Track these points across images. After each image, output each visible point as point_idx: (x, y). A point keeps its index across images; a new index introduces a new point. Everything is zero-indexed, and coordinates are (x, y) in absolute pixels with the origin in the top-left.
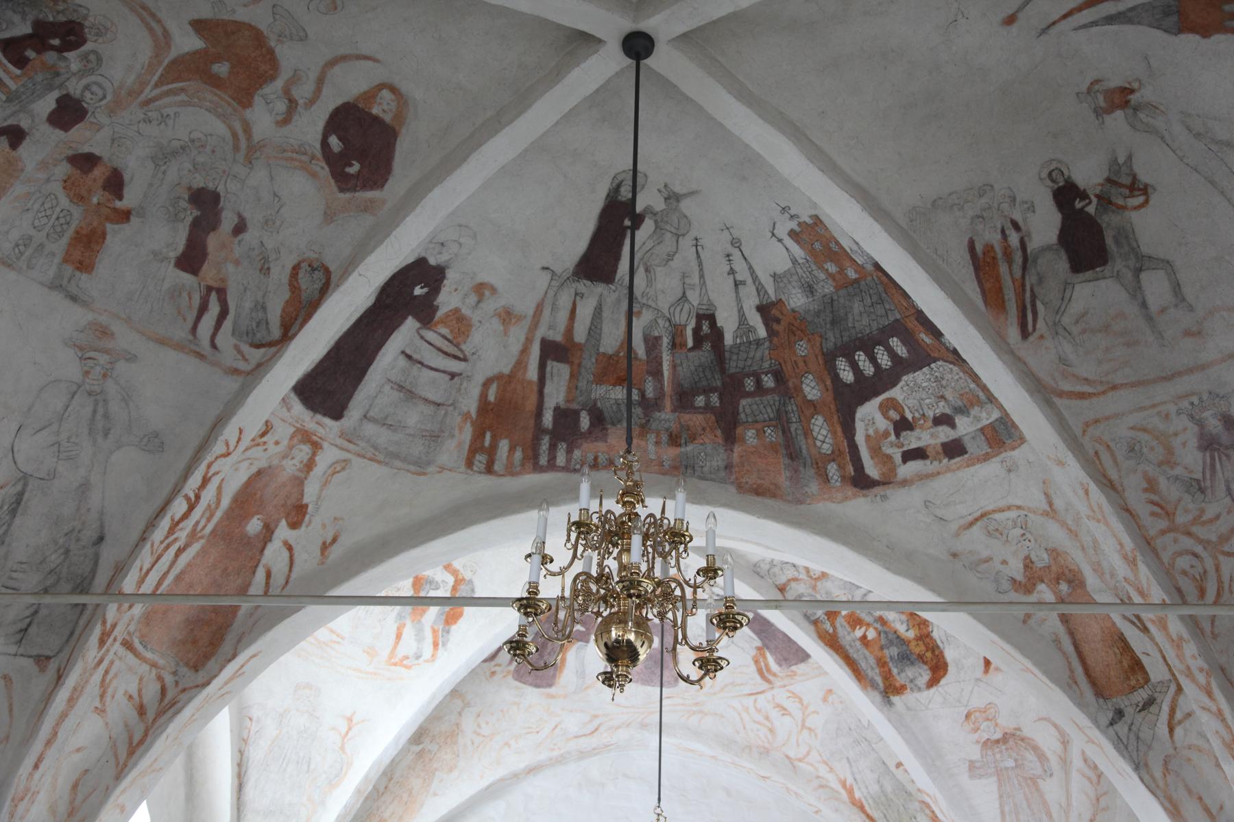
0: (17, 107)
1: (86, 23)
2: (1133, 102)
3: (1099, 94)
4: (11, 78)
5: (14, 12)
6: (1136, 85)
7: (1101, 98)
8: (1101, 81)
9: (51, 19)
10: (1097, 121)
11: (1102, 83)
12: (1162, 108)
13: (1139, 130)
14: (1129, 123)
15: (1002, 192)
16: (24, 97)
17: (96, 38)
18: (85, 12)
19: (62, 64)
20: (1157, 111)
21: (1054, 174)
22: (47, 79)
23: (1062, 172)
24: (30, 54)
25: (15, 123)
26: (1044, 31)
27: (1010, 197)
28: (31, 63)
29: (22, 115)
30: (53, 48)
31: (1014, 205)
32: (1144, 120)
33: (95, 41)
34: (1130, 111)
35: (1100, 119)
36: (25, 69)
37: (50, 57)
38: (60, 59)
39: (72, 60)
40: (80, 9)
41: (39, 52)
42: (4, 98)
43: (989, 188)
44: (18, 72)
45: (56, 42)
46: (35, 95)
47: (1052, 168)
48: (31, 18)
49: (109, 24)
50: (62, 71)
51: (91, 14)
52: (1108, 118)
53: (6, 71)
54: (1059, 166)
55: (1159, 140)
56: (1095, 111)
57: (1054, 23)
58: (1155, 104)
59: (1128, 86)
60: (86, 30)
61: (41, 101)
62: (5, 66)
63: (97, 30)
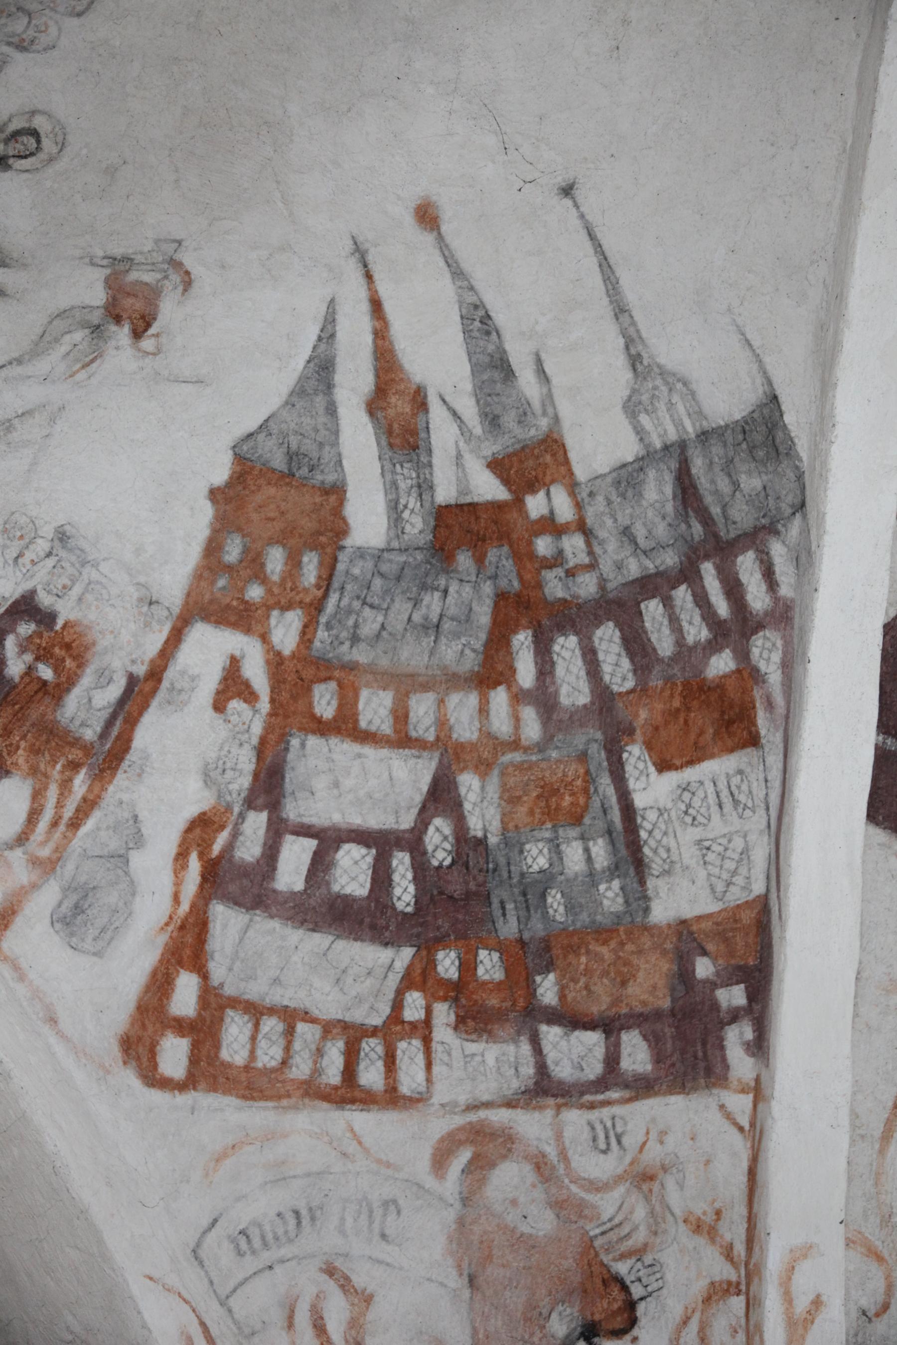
2: (113, 328)
3: (159, 276)
6: (147, 344)
7: (148, 277)
8: (185, 290)
10: (101, 253)
11: (181, 288)
12: (82, 375)
13: (50, 322)
14: (73, 308)
15: (53, 30)
20: (78, 366)
21: (31, 142)
23: (26, 157)
26: (360, 253)
27: (32, 42)
31: (9, 44)
32: (67, 337)
34: (96, 317)
35: (105, 262)
43: (79, 8)
47: (46, 143)
52: (98, 275)
54: (42, 156)
55: (15, 355)
56: (127, 259)
57: (369, 276)
58: (94, 365)
59: (151, 331)
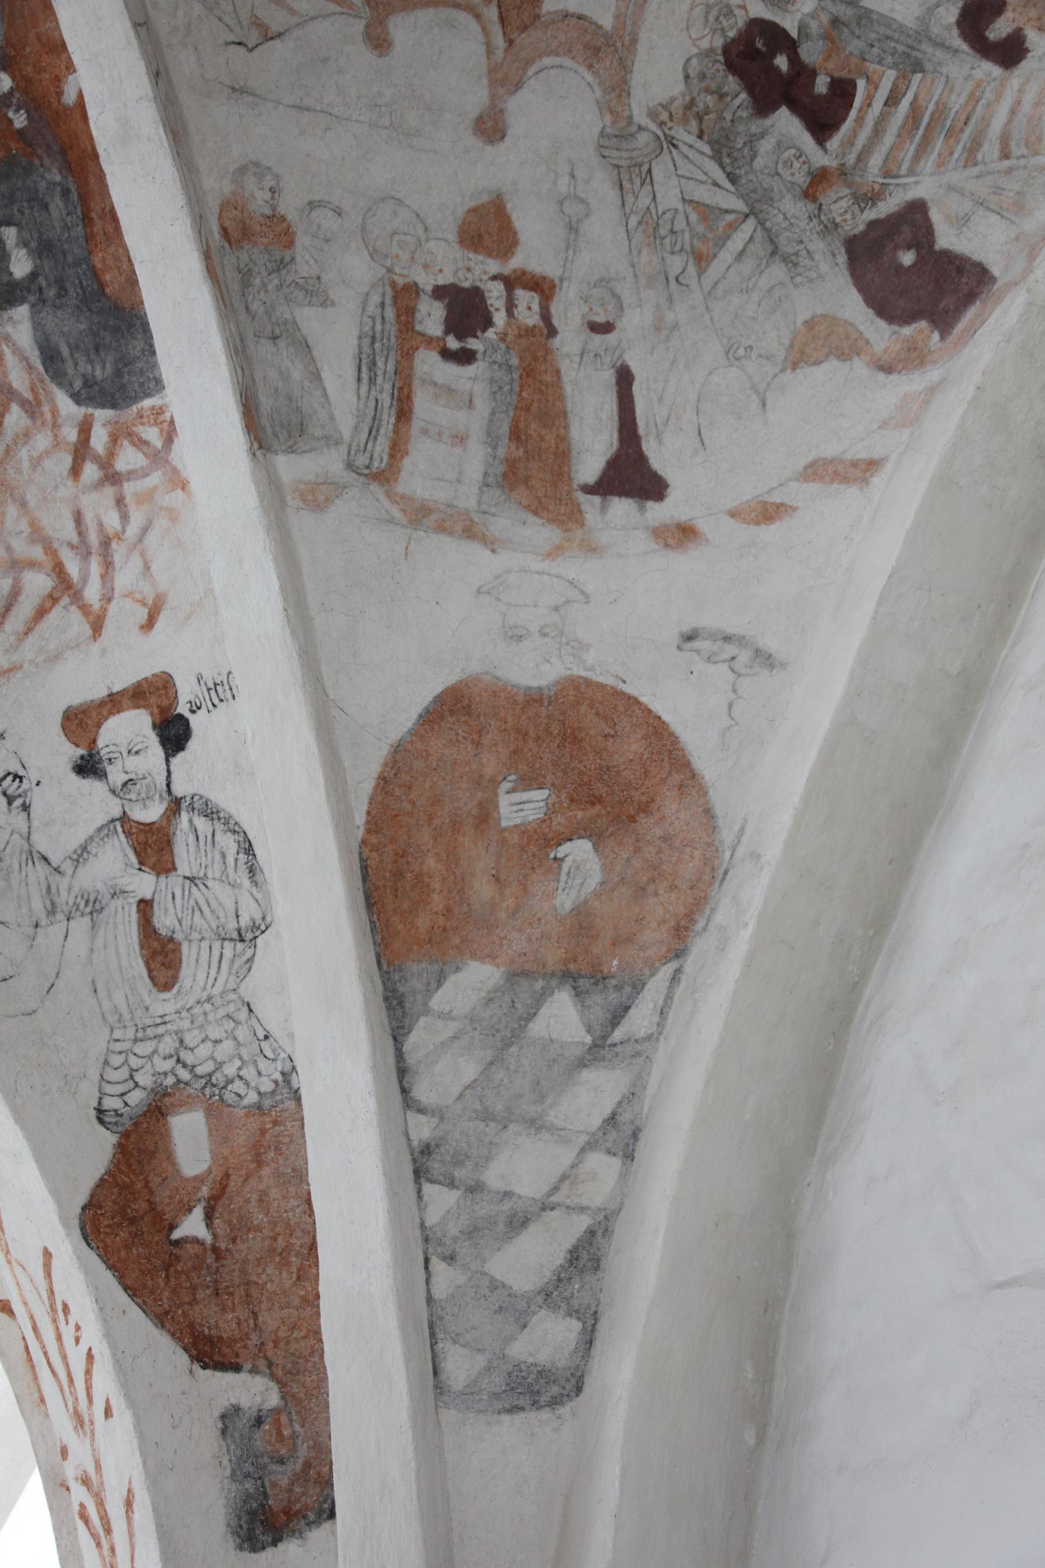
0: (924, 46)
1: (719, 42)
4: (876, 88)
5: (754, 156)
9: (743, 96)
16: (900, 48)
17: (736, 11)
18: (694, 62)
19: (814, 26)
22: (852, 33)
24: (821, 85)
25: (955, 32)
28: (836, 75)
29: (935, 30)
30: (794, 59)
33: (743, 7)
36: (852, 76)
37: (810, 53)
38: (807, 35)
39: (799, 16)
40: (692, 73)
41: (813, 74)
42: (919, 76)
44: (861, 84)
45: (782, 62)
46: (889, 33)
48: (756, 126)
49: (699, 11)
50: (825, 18)
51: (695, 51)
53: (868, 103)
60: (732, 34)
61: (894, 15)
62: (860, 110)
63: (722, 18)
